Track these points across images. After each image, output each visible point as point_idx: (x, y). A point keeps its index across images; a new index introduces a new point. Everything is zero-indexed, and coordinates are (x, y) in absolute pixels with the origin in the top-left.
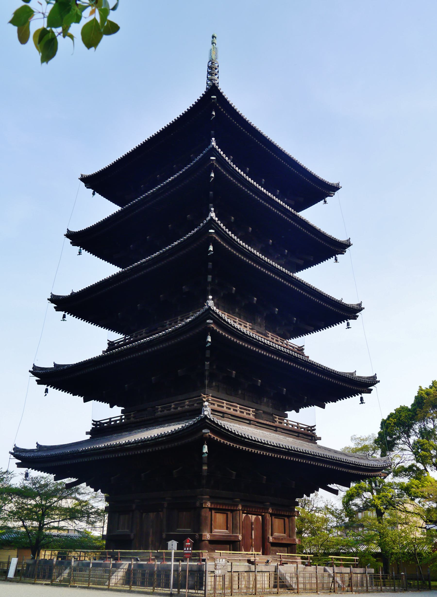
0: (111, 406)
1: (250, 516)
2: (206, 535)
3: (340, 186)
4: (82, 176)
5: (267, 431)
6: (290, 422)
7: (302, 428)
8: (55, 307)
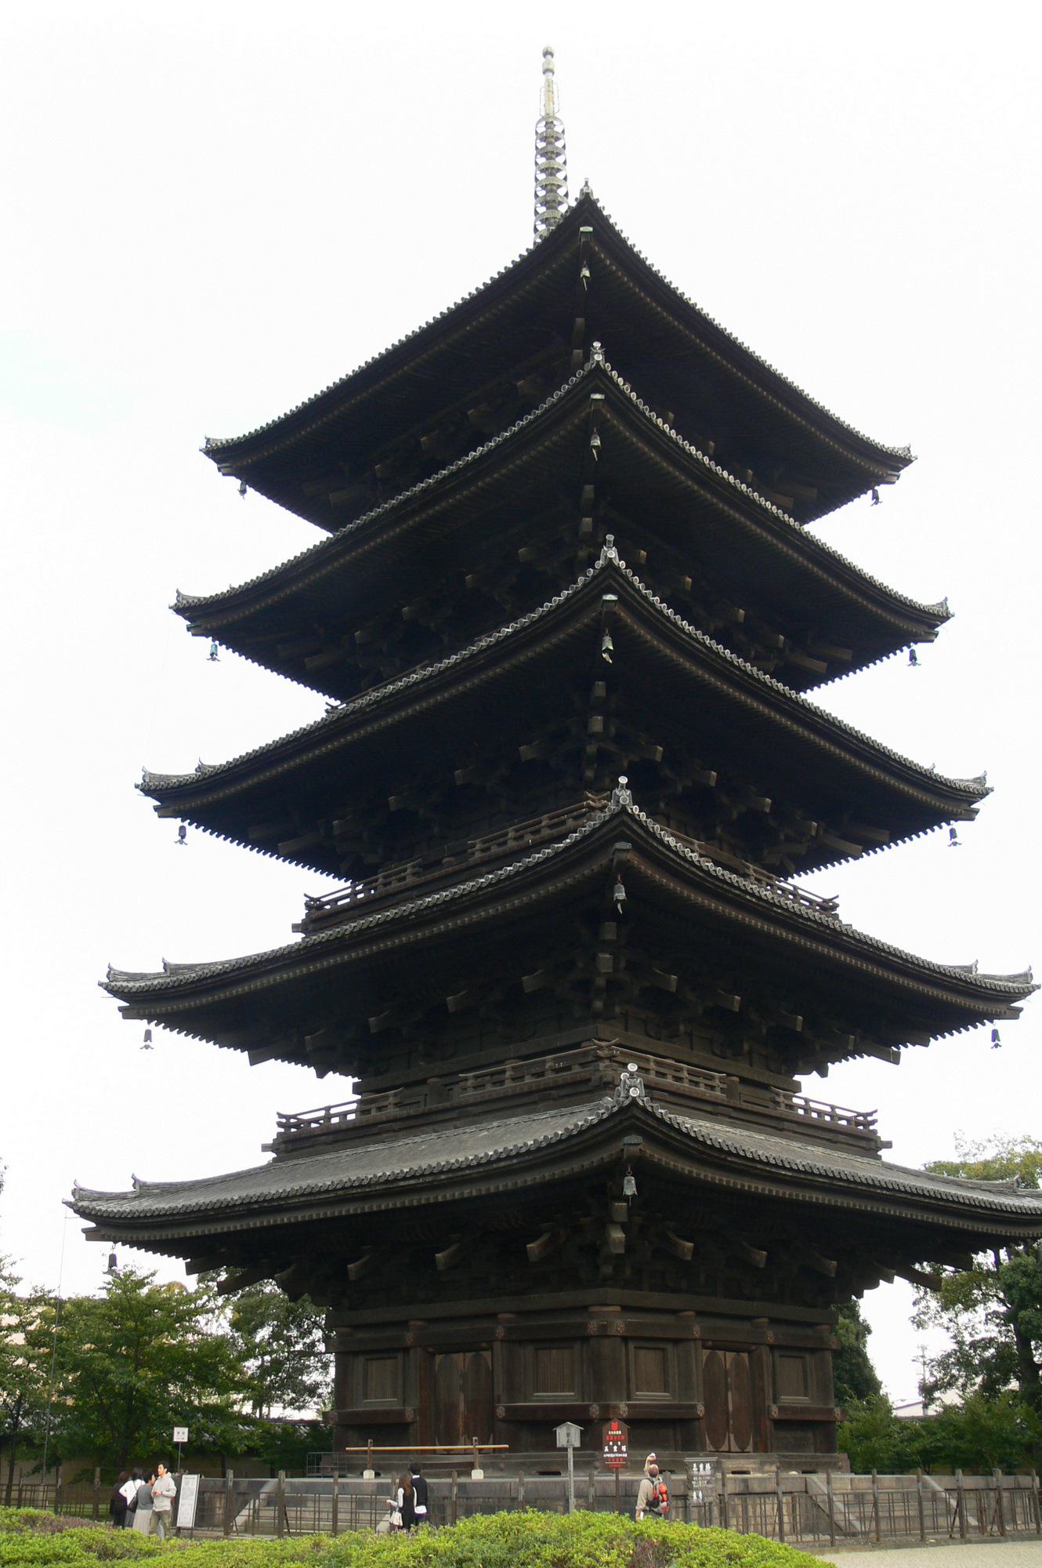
0: (321, 1074)
1: (720, 1353)
2: (616, 1407)
3: (913, 453)
4: (208, 440)
5: (760, 1132)
6: (812, 1105)
7: (841, 1118)
8: (156, 809)
